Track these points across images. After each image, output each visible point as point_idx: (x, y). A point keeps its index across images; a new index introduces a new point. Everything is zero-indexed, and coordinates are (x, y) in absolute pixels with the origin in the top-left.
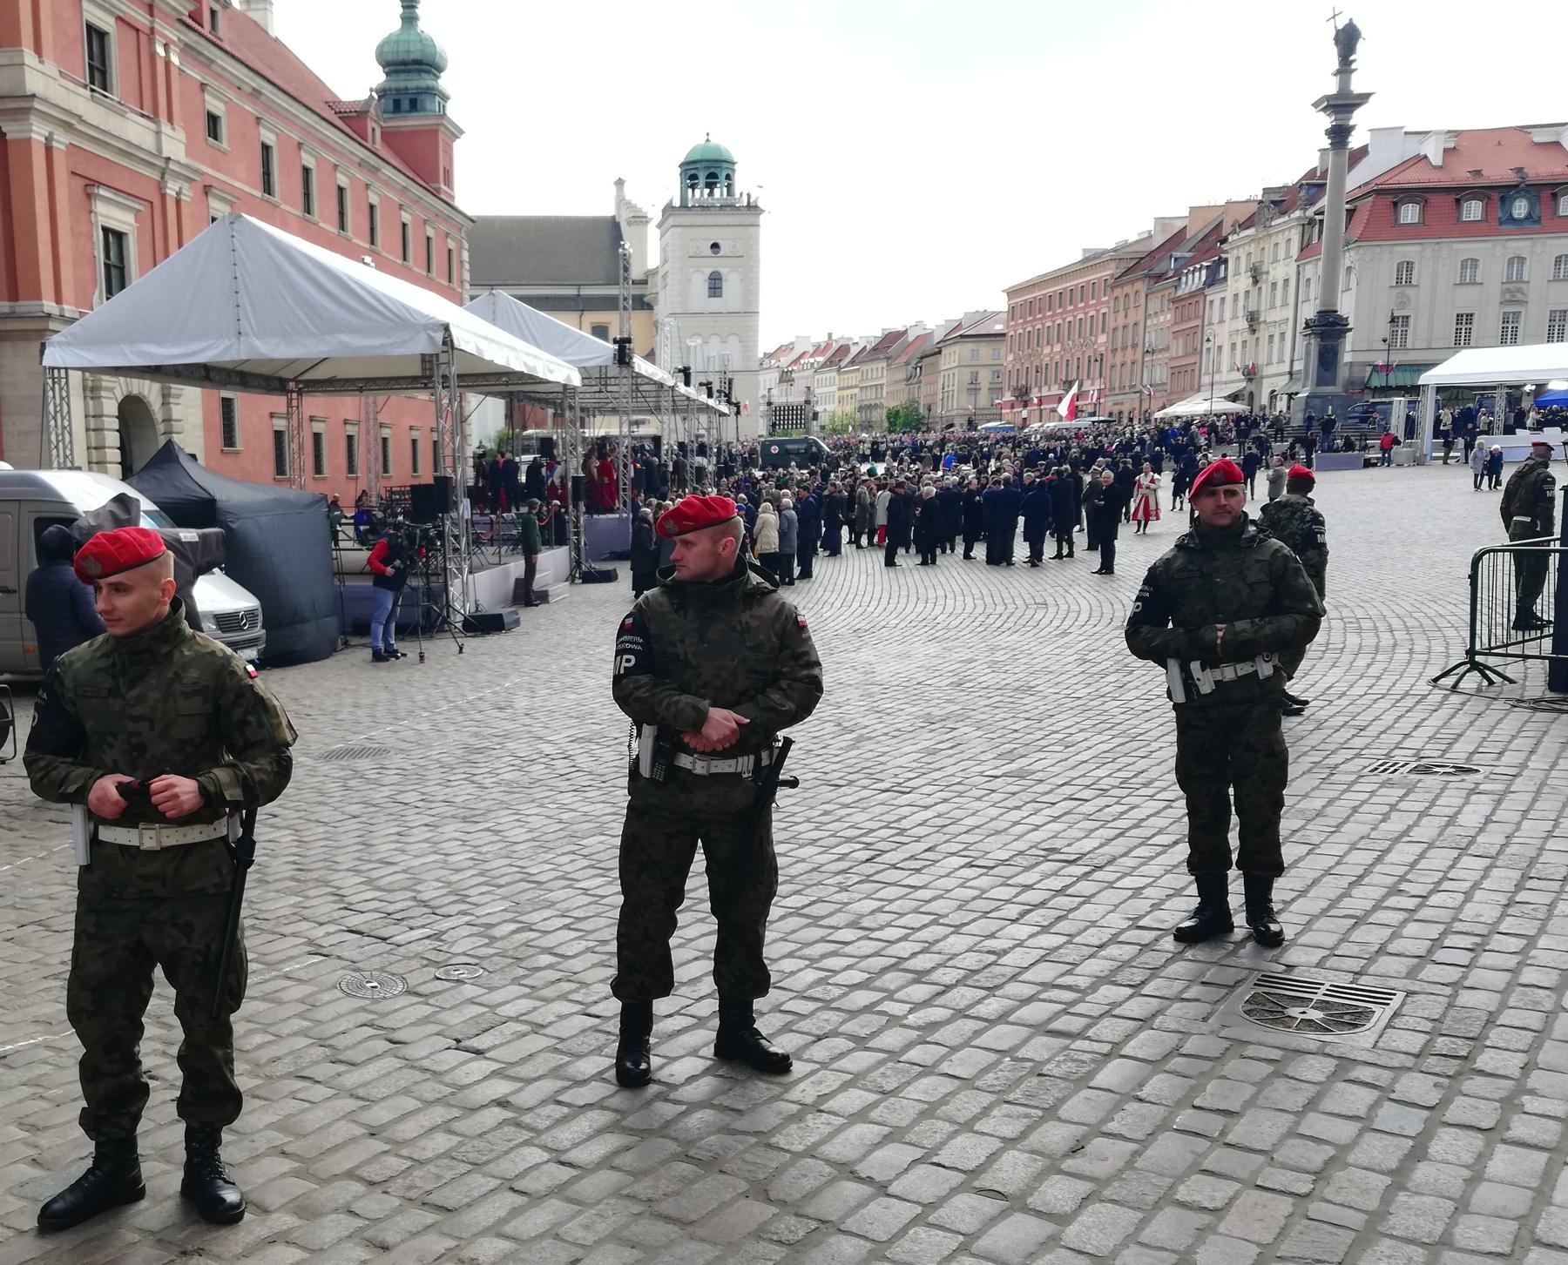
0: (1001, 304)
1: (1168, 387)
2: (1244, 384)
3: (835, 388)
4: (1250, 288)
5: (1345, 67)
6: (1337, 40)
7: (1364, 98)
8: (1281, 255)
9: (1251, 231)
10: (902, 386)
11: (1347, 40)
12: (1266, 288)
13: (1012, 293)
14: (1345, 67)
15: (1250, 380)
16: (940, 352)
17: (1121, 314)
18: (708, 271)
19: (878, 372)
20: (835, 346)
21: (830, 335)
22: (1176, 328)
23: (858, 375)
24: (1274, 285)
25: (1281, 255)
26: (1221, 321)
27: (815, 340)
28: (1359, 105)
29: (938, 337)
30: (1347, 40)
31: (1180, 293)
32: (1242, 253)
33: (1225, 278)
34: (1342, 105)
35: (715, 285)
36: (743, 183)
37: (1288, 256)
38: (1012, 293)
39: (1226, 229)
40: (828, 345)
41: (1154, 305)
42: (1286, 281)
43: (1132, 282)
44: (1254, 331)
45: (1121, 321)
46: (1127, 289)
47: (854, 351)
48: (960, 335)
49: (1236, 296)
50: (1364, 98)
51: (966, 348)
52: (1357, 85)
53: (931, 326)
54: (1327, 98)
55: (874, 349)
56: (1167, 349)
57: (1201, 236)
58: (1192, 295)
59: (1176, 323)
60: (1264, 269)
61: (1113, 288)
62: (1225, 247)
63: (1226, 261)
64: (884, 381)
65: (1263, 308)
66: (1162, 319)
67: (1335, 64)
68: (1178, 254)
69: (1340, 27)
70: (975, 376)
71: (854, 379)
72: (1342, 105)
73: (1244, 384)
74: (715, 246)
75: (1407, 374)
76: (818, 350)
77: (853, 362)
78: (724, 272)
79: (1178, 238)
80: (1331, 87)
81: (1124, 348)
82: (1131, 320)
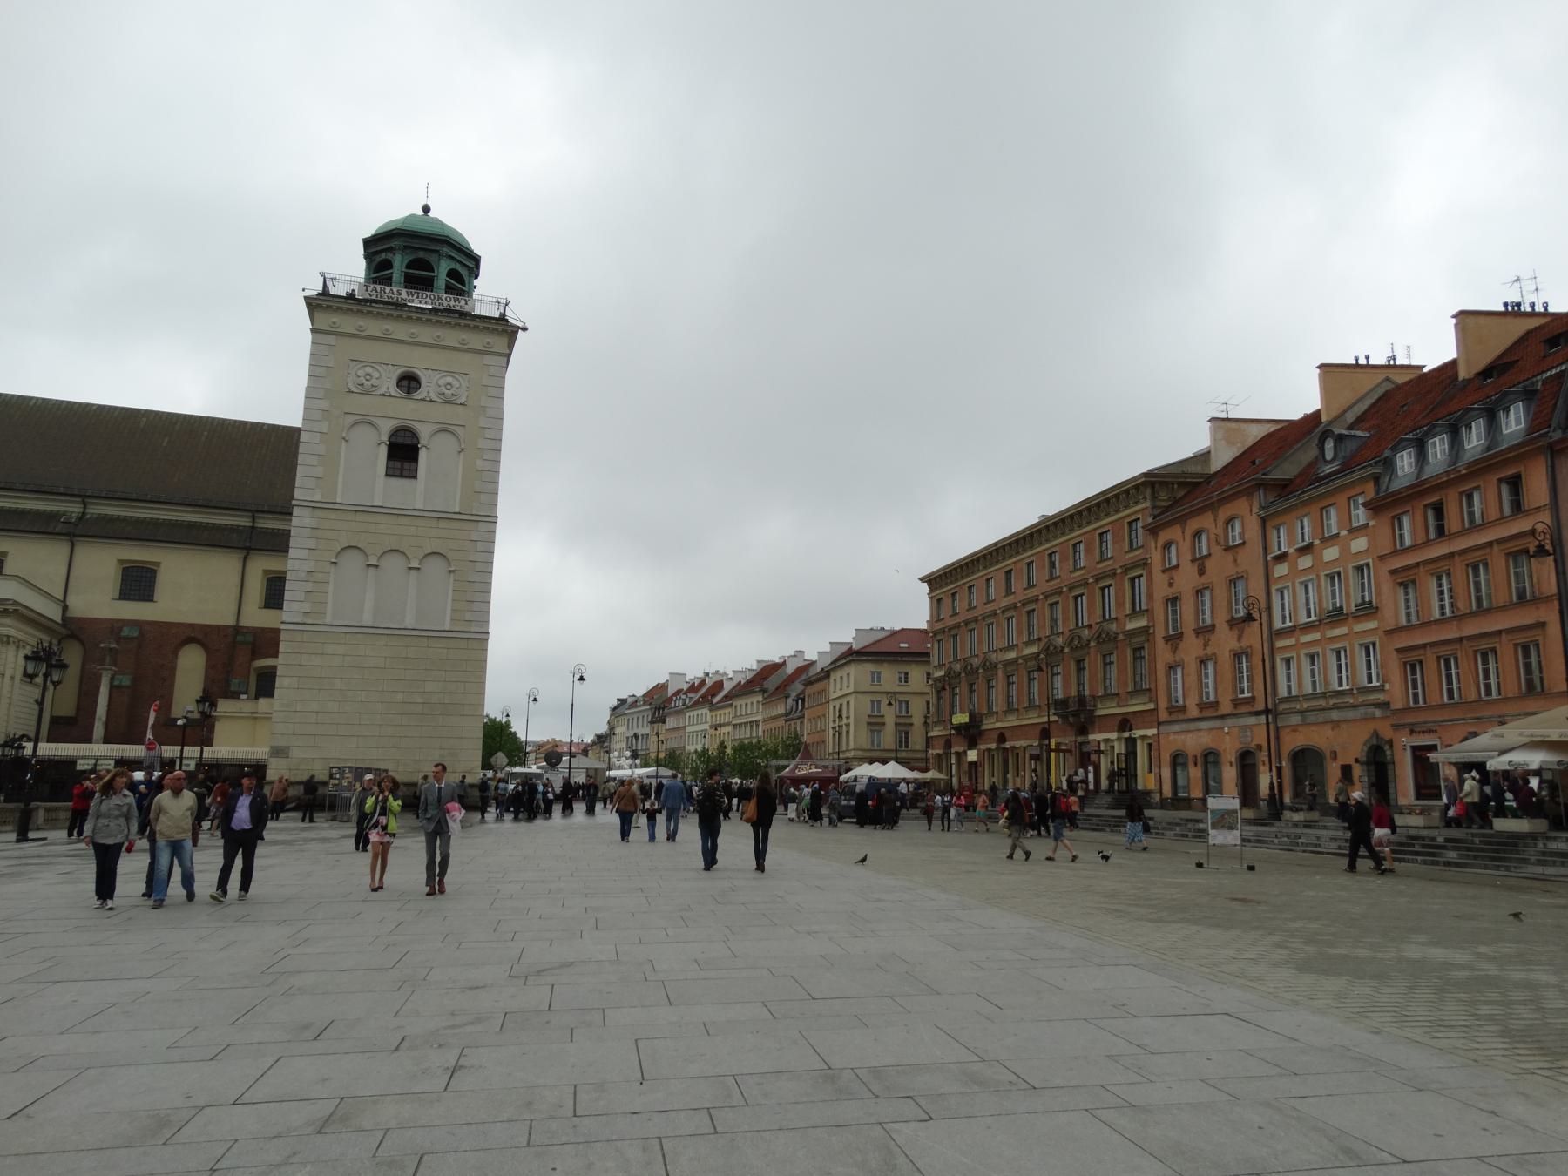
3: (706, 726)
18: (387, 427)
19: (753, 708)
20: (709, 682)
27: (690, 677)
35: (403, 452)
36: (486, 293)
38: (935, 581)
40: (703, 682)
47: (728, 686)
48: (850, 656)
51: (856, 675)
53: (811, 655)
55: (750, 682)
56: (1367, 610)
64: (759, 717)
66: (1331, 553)
71: (725, 715)
74: (409, 382)
76: (693, 688)
77: (726, 696)
78: (424, 431)
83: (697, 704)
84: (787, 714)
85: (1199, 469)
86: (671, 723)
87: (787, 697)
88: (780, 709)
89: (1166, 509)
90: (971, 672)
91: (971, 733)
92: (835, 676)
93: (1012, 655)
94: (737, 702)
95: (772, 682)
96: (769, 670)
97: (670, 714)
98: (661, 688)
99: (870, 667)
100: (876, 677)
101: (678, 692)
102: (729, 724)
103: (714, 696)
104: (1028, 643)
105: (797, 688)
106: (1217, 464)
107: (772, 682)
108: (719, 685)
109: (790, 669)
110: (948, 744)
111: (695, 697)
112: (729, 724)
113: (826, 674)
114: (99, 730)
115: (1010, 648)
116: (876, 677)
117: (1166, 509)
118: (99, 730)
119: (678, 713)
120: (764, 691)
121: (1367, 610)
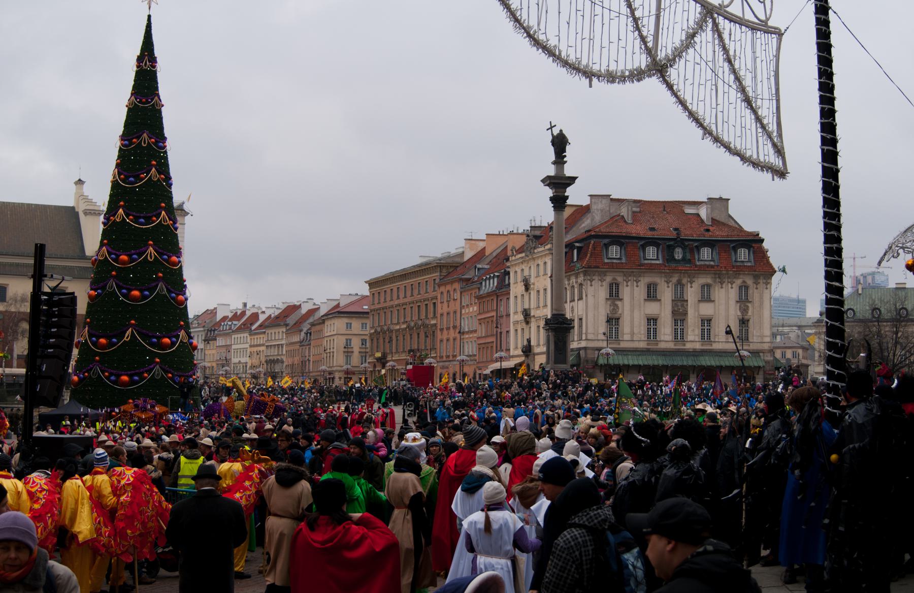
0: (365, 290)
1: (477, 358)
2: (523, 359)
3: (247, 346)
4: (524, 293)
5: (560, 159)
6: (554, 143)
7: (573, 179)
8: (541, 273)
9: (523, 255)
10: (297, 347)
11: (560, 143)
12: (533, 294)
13: (372, 284)
14: (560, 159)
15: (527, 356)
16: (324, 322)
17: (445, 304)
19: (279, 335)
20: (248, 314)
21: (245, 305)
22: (480, 317)
23: (265, 336)
24: (538, 291)
25: (541, 273)
26: (508, 315)
28: (569, 185)
29: (323, 311)
30: (560, 143)
31: (481, 292)
32: (518, 269)
33: (509, 284)
34: (559, 184)
37: (545, 274)
39: (509, 253)
40: (243, 313)
41: (466, 300)
42: (545, 290)
43: (452, 283)
44: (527, 323)
45: (445, 309)
46: (448, 287)
47: (262, 318)
48: (337, 312)
49: (516, 297)
50: (573, 179)
52: (568, 171)
54: (549, 177)
55: (277, 317)
56: (475, 331)
57: (494, 254)
58: (489, 295)
59: (480, 314)
60: (532, 280)
61: (439, 286)
62: (508, 264)
63: (508, 273)
64: (283, 342)
65: (532, 307)
66: (471, 309)
67: (553, 158)
68: (479, 266)
69: (555, 134)
70: (348, 341)
71: (261, 339)
72: (559, 184)
73: (523, 359)
75: (620, 357)
76: (236, 317)
77: (260, 326)
79: (480, 255)
80: (551, 171)
81: (448, 329)
82: (451, 310)
83: (240, 329)
84: (301, 342)
85: (458, 260)
86: (220, 341)
87: (301, 331)
88: (296, 338)
89: (445, 276)
90: (384, 333)
91: (383, 361)
92: (327, 323)
93: (398, 327)
94: (269, 331)
95: (291, 320)
96: (292, 309)
97: (220, 335)
98: (213, 312)
99: (346, 320)
100: (349, 326)
101: (224, 318)
102: (263, 345)
103: (252, 324)
104: (403, 323)
105: (306, 327)
106: (468, 256)
107: (291, 320)
108: (255, 316)
109: (304, 310)
110: (375, 366)
111: (238, 323)
112: (263, 345)
113: (323, 320)
114: (15, 363)
115: (398, 323)
116: (349, 326)
117: (445, 276)
118: (15, 363)
119: (227, 335)
120: (287, 325)
121: (475, 331)
